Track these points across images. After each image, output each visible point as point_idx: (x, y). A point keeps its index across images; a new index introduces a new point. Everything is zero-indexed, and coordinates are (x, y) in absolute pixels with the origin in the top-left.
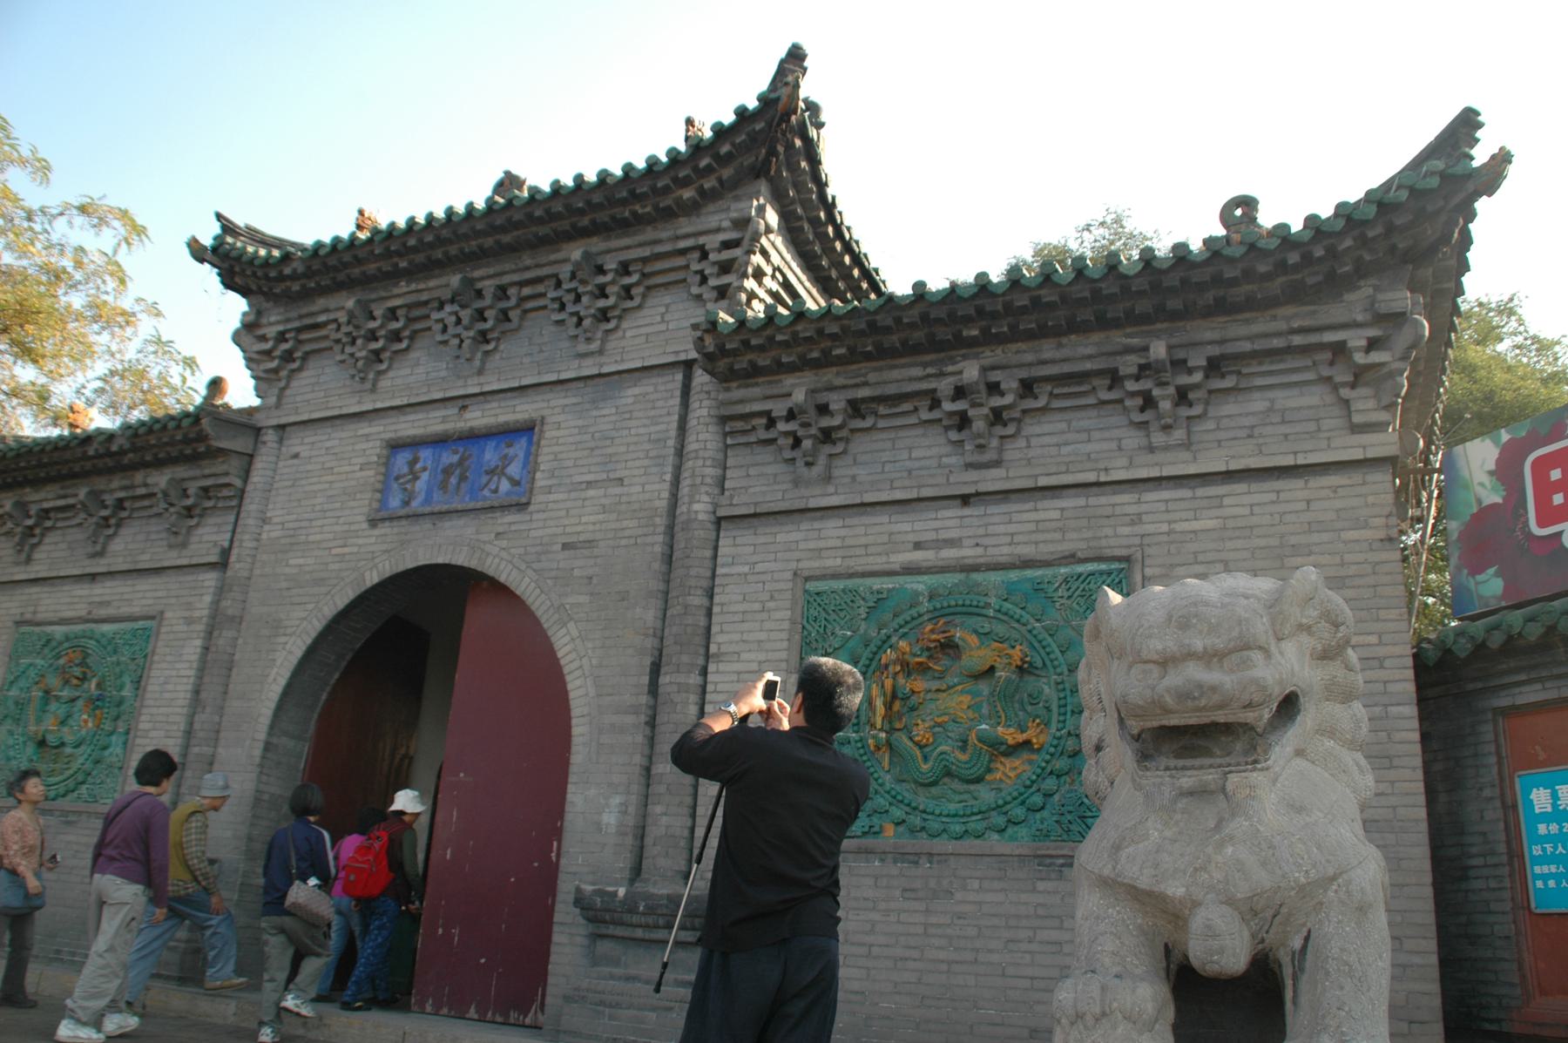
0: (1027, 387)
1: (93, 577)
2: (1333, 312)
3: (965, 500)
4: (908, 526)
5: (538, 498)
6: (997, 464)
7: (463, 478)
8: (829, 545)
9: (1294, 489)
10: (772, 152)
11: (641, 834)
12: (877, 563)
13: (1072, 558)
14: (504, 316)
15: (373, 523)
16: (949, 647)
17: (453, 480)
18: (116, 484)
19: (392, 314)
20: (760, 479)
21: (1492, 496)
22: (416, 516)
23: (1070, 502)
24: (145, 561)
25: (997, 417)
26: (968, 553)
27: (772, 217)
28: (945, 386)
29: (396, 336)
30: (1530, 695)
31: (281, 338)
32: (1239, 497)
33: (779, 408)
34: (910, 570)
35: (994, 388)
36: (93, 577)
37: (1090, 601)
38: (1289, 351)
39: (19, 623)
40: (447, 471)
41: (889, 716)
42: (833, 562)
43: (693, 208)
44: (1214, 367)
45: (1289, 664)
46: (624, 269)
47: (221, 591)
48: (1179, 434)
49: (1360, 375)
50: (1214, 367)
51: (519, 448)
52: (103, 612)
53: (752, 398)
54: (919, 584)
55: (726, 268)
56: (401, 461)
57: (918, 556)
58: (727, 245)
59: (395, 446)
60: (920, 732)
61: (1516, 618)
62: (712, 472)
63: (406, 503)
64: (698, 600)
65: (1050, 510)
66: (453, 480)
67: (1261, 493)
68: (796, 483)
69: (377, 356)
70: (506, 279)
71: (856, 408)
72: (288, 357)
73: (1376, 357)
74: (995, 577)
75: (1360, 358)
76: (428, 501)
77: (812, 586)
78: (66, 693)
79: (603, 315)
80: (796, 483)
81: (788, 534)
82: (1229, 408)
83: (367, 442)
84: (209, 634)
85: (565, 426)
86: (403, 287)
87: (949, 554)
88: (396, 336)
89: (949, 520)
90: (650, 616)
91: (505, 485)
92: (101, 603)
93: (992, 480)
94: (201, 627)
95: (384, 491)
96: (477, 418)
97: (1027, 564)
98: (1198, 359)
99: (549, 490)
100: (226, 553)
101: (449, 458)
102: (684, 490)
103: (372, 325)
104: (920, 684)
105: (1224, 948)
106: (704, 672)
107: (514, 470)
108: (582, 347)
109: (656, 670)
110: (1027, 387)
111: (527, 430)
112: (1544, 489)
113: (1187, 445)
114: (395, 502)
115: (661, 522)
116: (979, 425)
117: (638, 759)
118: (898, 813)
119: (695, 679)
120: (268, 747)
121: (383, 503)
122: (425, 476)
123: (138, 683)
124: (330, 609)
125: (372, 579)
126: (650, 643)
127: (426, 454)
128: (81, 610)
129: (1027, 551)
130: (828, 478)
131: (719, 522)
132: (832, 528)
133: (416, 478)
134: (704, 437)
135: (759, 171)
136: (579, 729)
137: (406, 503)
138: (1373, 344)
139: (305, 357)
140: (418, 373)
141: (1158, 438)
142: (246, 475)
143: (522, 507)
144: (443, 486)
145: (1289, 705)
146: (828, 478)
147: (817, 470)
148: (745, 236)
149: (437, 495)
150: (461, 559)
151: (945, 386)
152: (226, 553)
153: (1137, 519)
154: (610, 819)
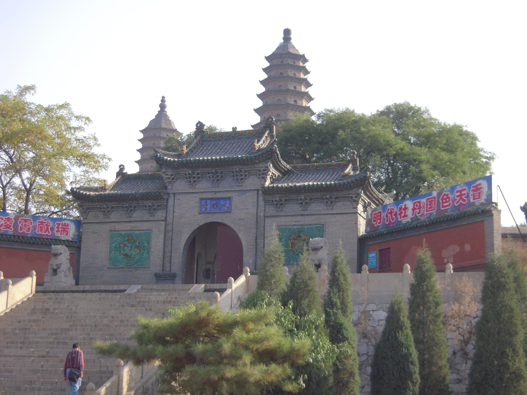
0: (311, 199)
1: (130, 222)
2: (351, 192)
3: (302, 215)
4: (294, 219)
5: (233, 211)
6: (306, 210)
7: (217, 206)
8: (282, 221)
9: (345, 216)
10: (272, 157)
11: (255, 263)
12: (290, 224)
13: (316, 224)
14: (222, 177)
15: (200, 214)
16: (300, 236)
17: (215, 207)
18: (134, 203)
19: (198, 174)
20: (271, 210)
21: (370, 218)
22: (209, 213)
23: (316, 216)
24: (145, 219)
25: (306, 203)
26: (302, 223)
27: (271, 165)
28: (299, 198)
29: (199, 178)
30: (370, 243)
31: (172, 175)
32: (338, 217)
33: (274, 200)
34: (294, 225)
35: (306, 199)
36: (130, 222)
37: (309, 239)
38: (345, 197)
39: (111, 231)
40: (214, 205)
41: (292, 246)
42: (283, 224)
43: (258, 163)
44: (336, 198)
45: (322, 244)
46: (245, 171)
47: (166, 225)
48: (331, 207)
49: (354, 201)
50: (336, 198)
51: (228, 202)
52: (135, 229)
53: (270, 198)
54: (295, 227)
55: (263, 174)
56: (203, 202)
57: (295, 223)
58: (264, 170)
59: (202, 199)
60: (296, 248)
61: (372, 233)
62: (263, 208)
63: (206, 210)
64: (262, 229)
65: (313, 217)
66: (215, 207)
67: (340, 216)
68: (277, 211)
69: (195, 181)
70: (222, 170)
71: (286, 200)
72: (173, 179)
73: (356, 199)
74: (306, 226)
75: (354, 199)
76: (210, 210)
77: (280, 227)
78: (129, 245)
79: (242, 179)
80: (277, 211)
81: (276, 219)
82: (338, 204)
83: (196, 198)
84: (165, 233)
85: (236, 199)
86: (200, 169)
87: (300, 223)
88: (199, 178)
89: (299, 218)
90: (255, 231)
91: (226, 208)
92: (134, 227)
93: (306, 213)
94: (163, 232)
95: (201, 207)
96: (219, 195)
97: (310, 225)
98: (334, 197)
99: (235, 210)
100: (166, 217)
101: (213, 202)
102: (259, 211)
103: (194, 176)
104: (296, 241)
105: (317, 263)
106: (264, 240)
107: (227, 205)
108: (238, 185)
109: (256, 240)
110: (311, 199)
111: (229, 198)
112: (374, 217)
113: (332, 209)
114: (203, 210)
115: (255, 216)
116: (304, 205)
117: (254, 253)
118: (293, 259)
119: (263, 241)
120: (183, 253)
121: (201, 210)
122: (209, 205)
123: (149, 243)
124: (193, 229)
125: (201, 224)
126: (255, 235)
127: (208, 201)
128: (129, 228)
129: (310, 223)
130: (282, 211)
131: (265, 217)
132: (283, 219)
133: (207, 205)
134: (261, 203)
135: (270, 158)
136: (244, 248)
137: (206, 210)
138: (356, 197)
139: (177, 179)
140: (204, 185)
141: (328, 208)
142: (167, 203)
143: (230, 212)
144: (213, 207)
145: (322, 247)
146: (282, 211)
147: (280, 209)
148: (267, 169)
149: (212, 209)
150: (219, 221)
151: (299, 198)
152: (166, 217)
153: (325, 219)
154: (251, 261)
